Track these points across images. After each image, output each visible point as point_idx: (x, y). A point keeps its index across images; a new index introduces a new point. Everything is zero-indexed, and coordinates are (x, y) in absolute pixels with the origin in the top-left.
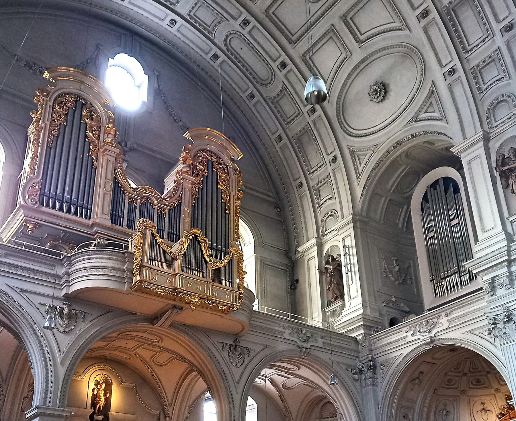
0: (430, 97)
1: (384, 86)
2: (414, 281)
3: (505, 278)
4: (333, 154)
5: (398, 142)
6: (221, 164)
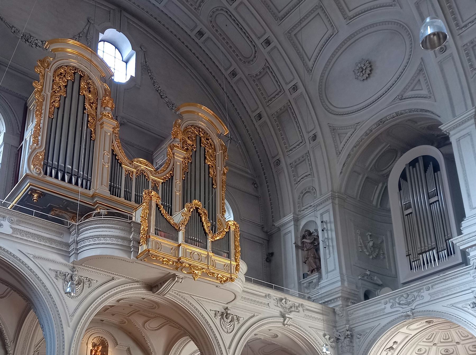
4: (313, 132)
6: (208, 139)
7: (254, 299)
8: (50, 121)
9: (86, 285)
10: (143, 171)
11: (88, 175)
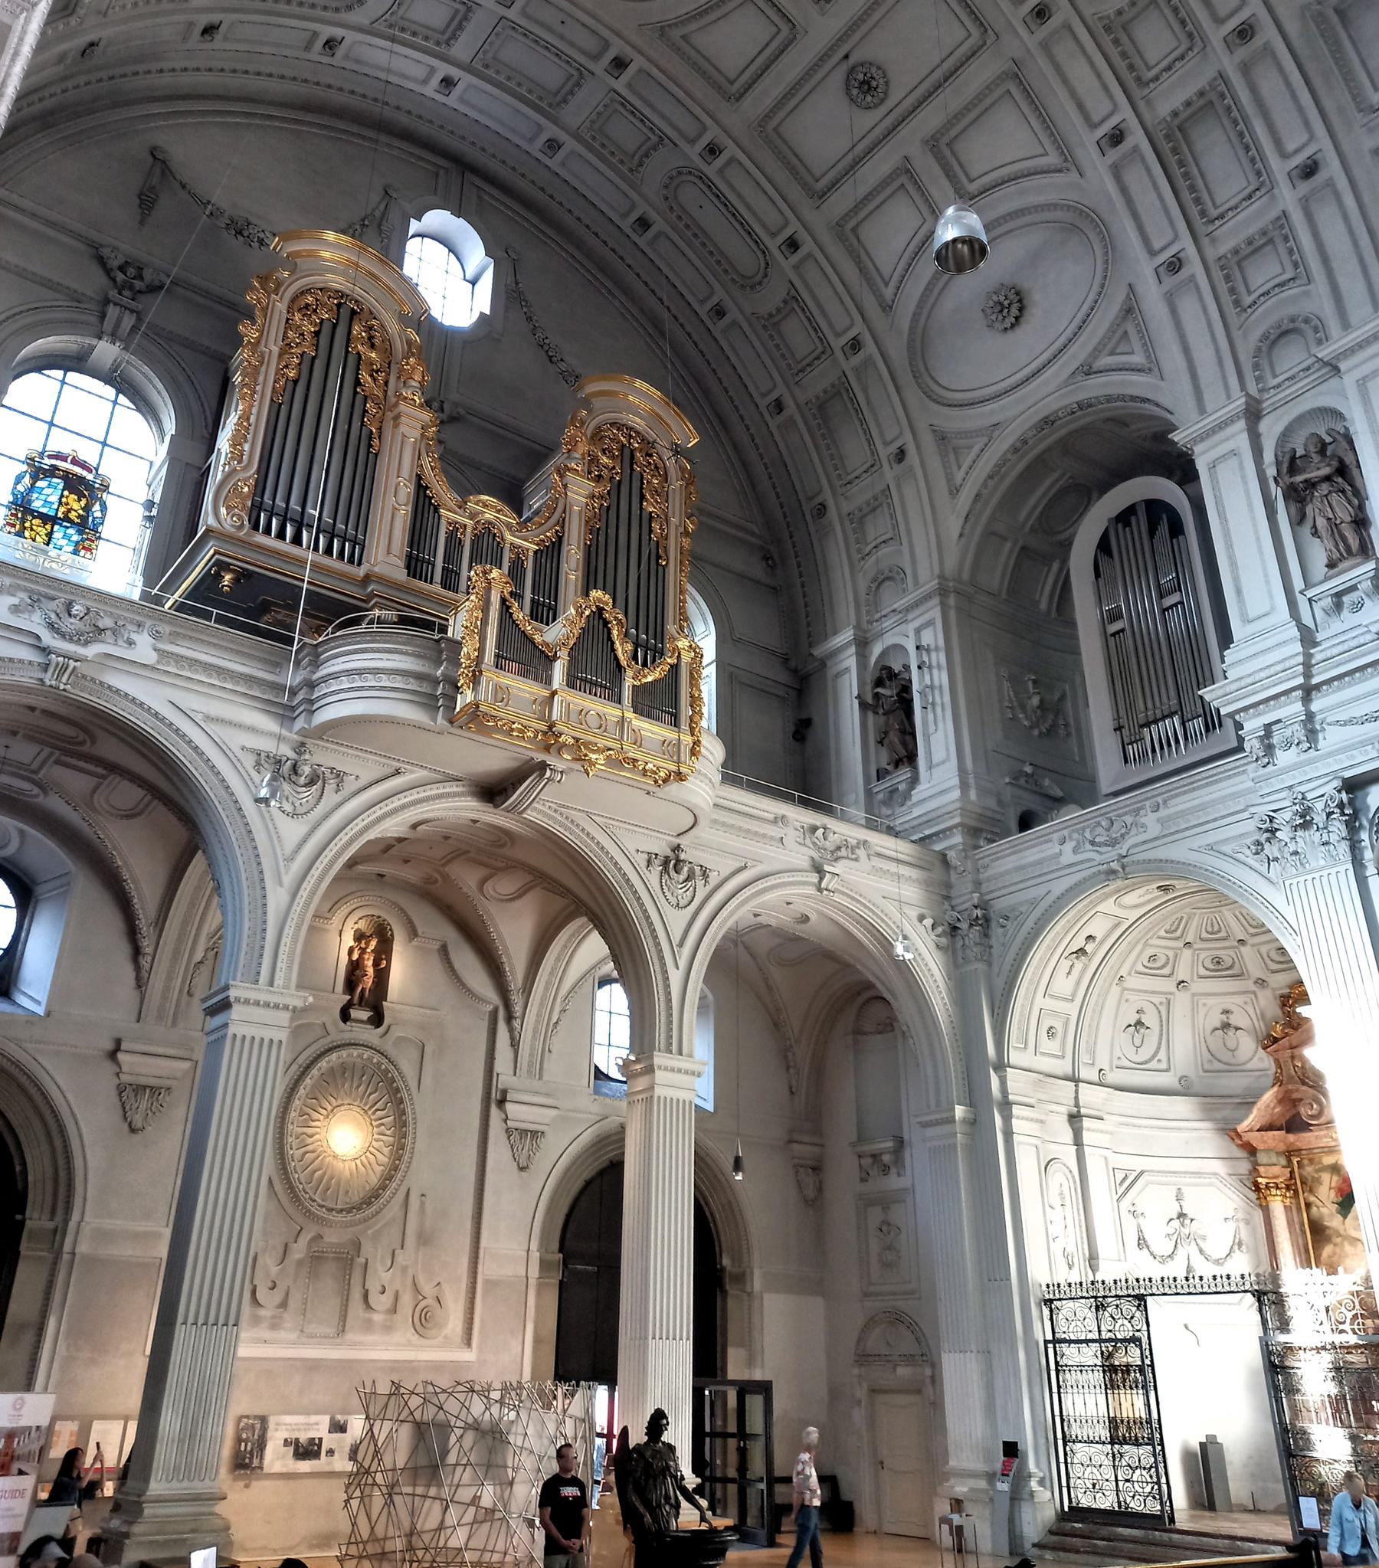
0: (1124, 319)
1: (1017, 294)
2: (1073, 732)
3: (1297, 727)
4: (898, 444)
5: (1046, 417)
6: (651, 456)
8: (275, 410)
9: (330, 787)
10: (490, 523)
11: (346, 526)
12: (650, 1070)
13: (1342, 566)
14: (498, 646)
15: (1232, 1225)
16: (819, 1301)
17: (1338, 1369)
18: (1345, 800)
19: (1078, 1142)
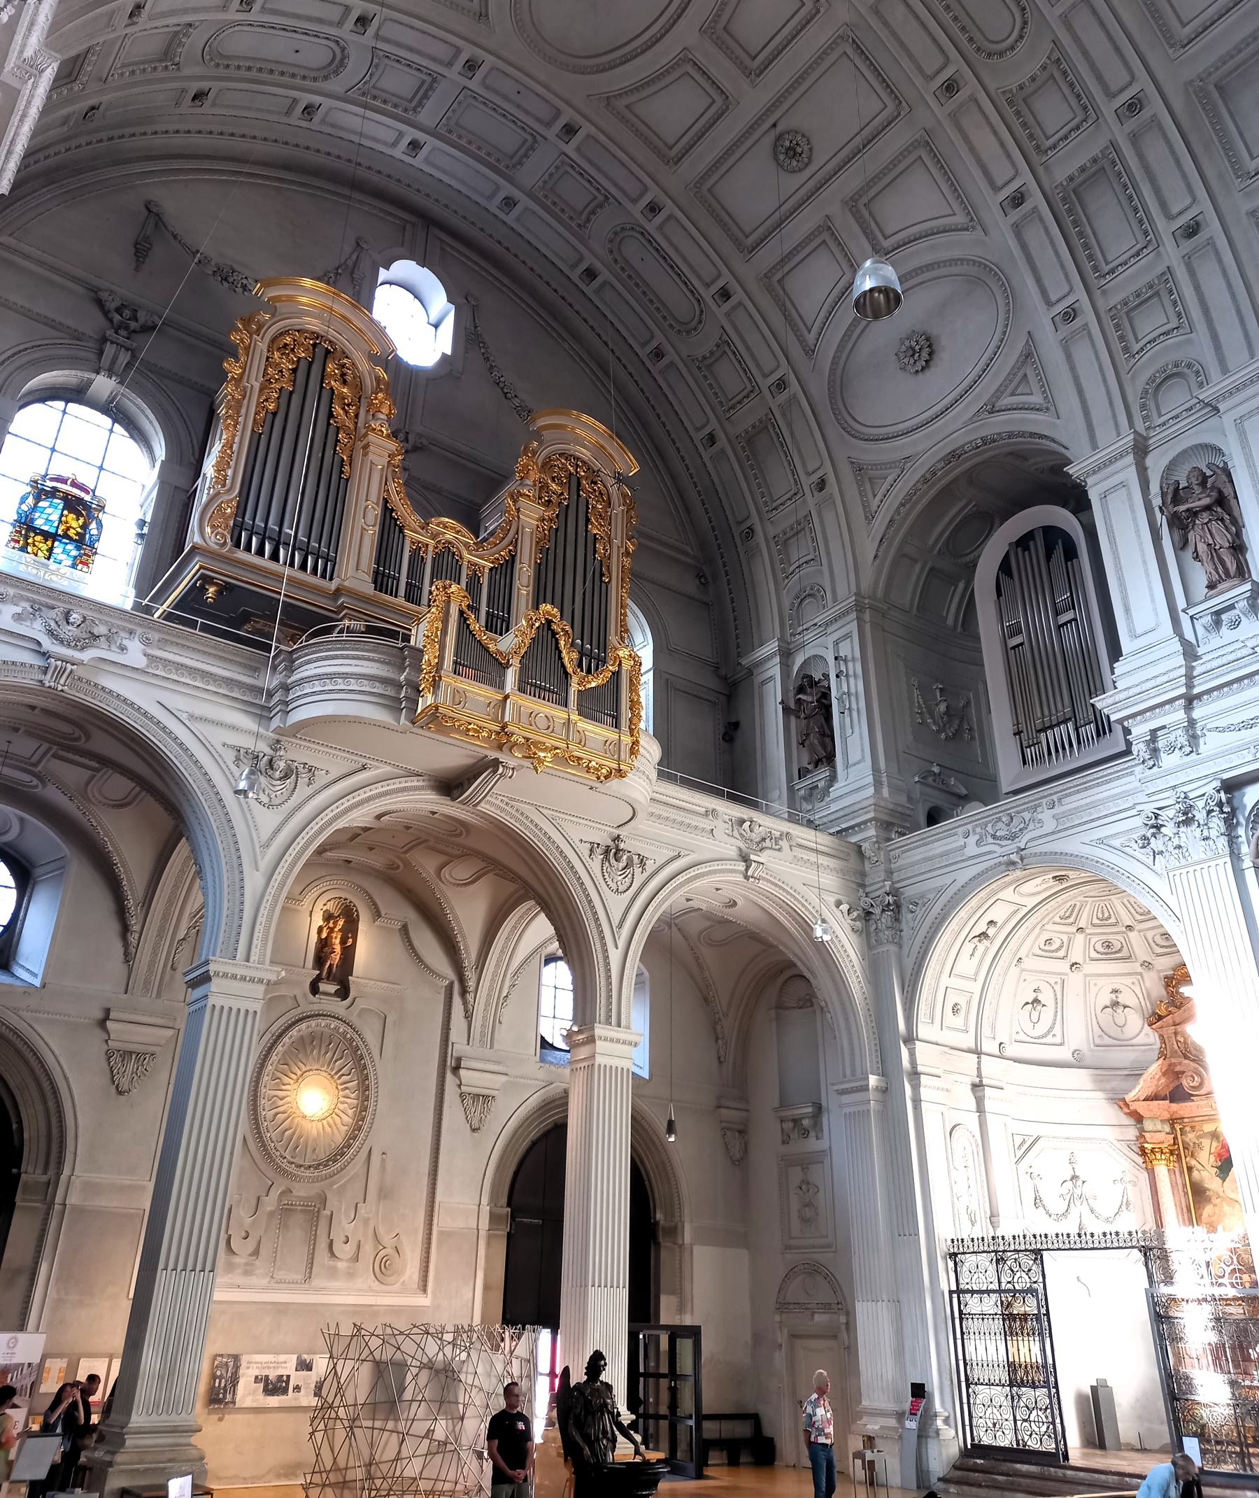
0: (1024, 362)
1: (928, 339)
3: (1179, 732)
4: (820, 474)
5: (954, 451)
6: (596, 483)
7: (679, 819)
9: (303, 781)
10: (450, 543)
12: (591, 1040)
13: (1221, 587)
14: (456, 655)
15: (1119, 1187)
16: (744, 1253)
17: (1218, 1320)
18: (1224, 799)
19: (980, 1109)
